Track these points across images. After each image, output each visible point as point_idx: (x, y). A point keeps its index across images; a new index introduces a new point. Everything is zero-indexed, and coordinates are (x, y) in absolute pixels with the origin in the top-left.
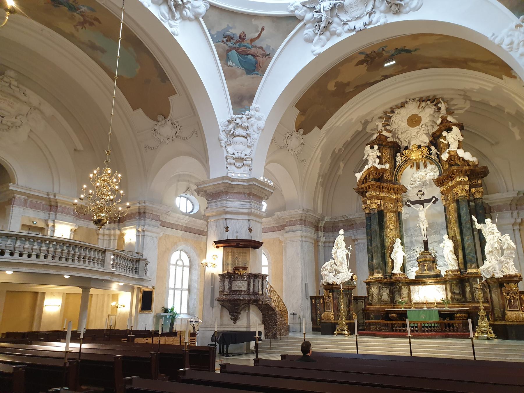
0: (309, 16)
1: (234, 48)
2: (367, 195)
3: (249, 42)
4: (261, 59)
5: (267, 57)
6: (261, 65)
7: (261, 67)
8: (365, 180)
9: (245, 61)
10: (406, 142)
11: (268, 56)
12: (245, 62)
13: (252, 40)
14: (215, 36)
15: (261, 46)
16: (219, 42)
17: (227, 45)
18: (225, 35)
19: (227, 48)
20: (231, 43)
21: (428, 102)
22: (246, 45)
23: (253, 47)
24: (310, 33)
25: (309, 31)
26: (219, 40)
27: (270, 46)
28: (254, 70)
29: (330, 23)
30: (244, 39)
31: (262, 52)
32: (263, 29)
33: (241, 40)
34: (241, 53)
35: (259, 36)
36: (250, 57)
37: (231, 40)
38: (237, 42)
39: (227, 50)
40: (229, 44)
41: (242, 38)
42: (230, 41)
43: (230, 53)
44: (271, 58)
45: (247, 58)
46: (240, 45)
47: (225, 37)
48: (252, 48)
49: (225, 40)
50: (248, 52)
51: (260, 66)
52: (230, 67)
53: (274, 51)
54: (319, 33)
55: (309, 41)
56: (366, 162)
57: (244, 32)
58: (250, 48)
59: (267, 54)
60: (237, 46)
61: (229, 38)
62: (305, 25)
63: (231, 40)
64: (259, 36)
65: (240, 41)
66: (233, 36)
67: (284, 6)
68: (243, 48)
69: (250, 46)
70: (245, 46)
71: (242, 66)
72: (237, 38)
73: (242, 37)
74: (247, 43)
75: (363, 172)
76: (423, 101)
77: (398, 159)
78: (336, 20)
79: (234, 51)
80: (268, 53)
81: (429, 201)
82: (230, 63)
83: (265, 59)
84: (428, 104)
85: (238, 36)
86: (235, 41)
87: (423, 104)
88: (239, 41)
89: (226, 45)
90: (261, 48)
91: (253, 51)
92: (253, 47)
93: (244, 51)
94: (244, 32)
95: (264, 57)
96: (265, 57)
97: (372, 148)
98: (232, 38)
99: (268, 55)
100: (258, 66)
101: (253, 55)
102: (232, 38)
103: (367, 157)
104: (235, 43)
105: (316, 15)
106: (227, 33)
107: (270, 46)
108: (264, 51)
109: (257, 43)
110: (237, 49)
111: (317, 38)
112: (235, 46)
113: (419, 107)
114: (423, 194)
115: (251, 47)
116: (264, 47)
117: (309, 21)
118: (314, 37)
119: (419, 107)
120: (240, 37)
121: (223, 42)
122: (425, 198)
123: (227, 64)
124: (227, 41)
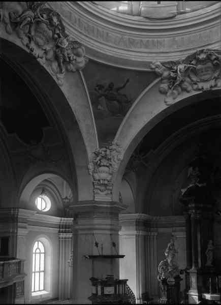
0: (166, 74)
1: (103, 95)
11: (129, 103)
13: (118, 89)
17: (98, 92)
24: (164, 87)
25: (164, 86)
29: (182, 82)
32: (128, 81)
35: (124, 86)
38: (106, 90)
40: (100, 91)
41: (111, 86)
43: (100, 99)
44: (132, 104)
47: (98, 86)
49: (97, 88)
54: (173, 88)
55: (164, 93)
59: (129, 100)
61: (100, 87)
62: (162, 79)
64: (124, 86)
67: (147, 64)
72: (106, 87)
78: (188, 79)
82: (99, 107)
85: (107, 85)
90: (125, 95)
101: (118, 101)
102: (103, 87)
105: (172, 74)
109: (121, 91)
110: (106, 96)
111: (170, 91)
117: (165, 78)
118: (168, 90)
121: (96, 90)
124: (99, 89)
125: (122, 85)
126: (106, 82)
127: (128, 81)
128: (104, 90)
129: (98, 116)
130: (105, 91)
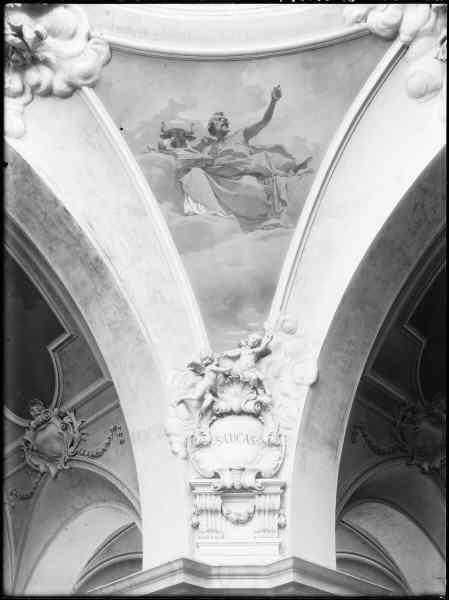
1: (197, 163)
3: (240, 138)
4: (282, 181)
5: (300, 171)
6: (283, 197)
7: (284, 203)
9: (233, 193)
12: (236, 196)
13: (249, 133)
14: (138, 136)
15: (278, 143)
16: (150, 150)
17: (176, 156)
18: (168, 128)
19: (176, 164)
20: (190, 151)
22: (232, 150)
23: (255, 150)
26: (151, 146)
27: (305, 140)
28: (265, 215)
30: (225, 133)
31: (285, 160)
32: (277, 94)
33: (215, 138)
34: (221, 173)
35: (268, 116)
36: (248, 181)
37: (187, 142)
39: (178, 171)
40: (180, 151)
42: (183, 144)
43: (185, 179)
45: (239, 184)
46: (213, 153)
47: (167, 135)
48: (251, 154)
49: (167, 142)
50: (242, 169)
51: (280, 199)
52: (190, 219)
53: (320, 150)
57: (221, 114)
58: (245, 156)
59: (299, 162)
60: (206, 156)
61: (180, 137)
63: (187, 142)
64: (268, 116)
65: (213, 141)
66: (189, 130)
68: (224, 160)
69: (242, 149)
70: (229, 152)
71: (228, 210)
72: (202, 132)
73: (218, 128)
74: (234, 143)
79: (197, 173)
80: (300, 159)
82: (189, 206)
83: (296, 178)
85: (206, 125)
86: (197, 142)
88: (210, 141)
89: (171, 158)
90: (279, 149)
91: (256, 161)
92: (255, 150)
93: (229, 166)
94: (221, 114)
95: (292, 172)
96: (296, 171)
98: (190, 137)
99: (303, 165)
100: (276, 201)
101: (258, 175)
102: (190, 137)
104: (200, 148)
106: (173, 122)
107: (305, 140)
108: (289, 156)
109: (264, 138)
110: (207, 166)
112: (199, 156)
115: (246, 153)
116: (288, 145)
120: (212, 130)
121: (162, 148)
123: (181, 211)
124: (174, 145)
125: (261, 114)
126: (198, 118)
127: (277, 94)
128: (190, 144)
129: (189, 239)
130: (200, 148)
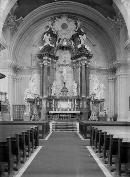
2: (44, 58)
8: (43, 50)
10: (60, 36)
21: (72, 19)
56: (44, 42)
75: (43, 46)
76: (69, 18)
77: (57, 43)
81: (67, 65)
84: (71, 20)
87: (69, 19)
97: (47, 35)
103: (45, 40)
113: (67, 20)
114: (66, 62)
119: (67, 20)
122: (66, 64)
